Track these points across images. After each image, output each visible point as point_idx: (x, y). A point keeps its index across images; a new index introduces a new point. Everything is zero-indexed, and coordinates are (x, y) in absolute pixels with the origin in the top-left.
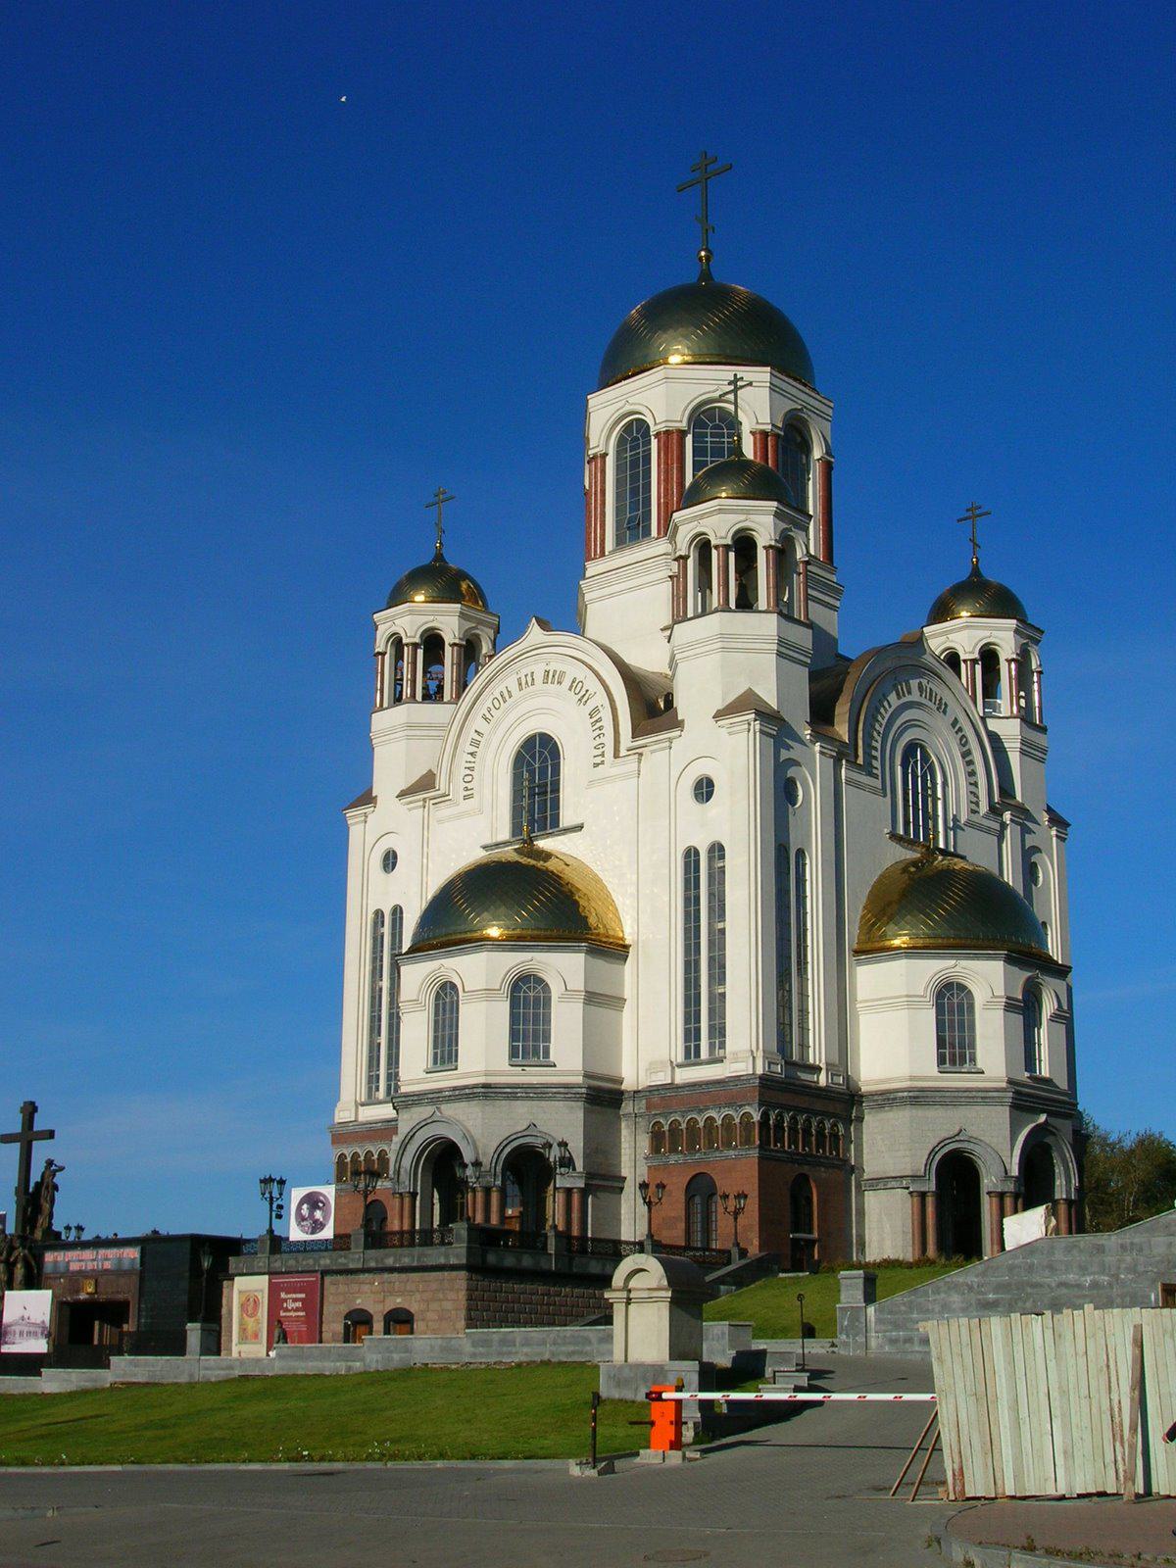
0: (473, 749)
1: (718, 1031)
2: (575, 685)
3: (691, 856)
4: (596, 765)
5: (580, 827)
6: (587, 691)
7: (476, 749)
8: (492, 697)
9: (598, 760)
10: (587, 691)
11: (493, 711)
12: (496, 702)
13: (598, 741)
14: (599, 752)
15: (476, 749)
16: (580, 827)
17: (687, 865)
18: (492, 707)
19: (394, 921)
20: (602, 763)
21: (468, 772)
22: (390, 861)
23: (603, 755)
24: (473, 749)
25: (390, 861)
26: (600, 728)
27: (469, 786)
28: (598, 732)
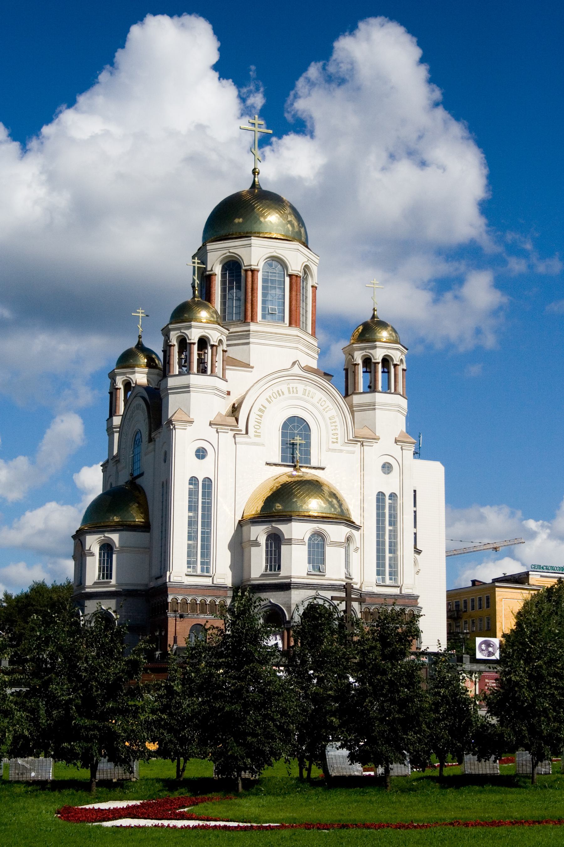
0: (260, 413)
1: (394, 574)
2: (321, 401)
3: (380, 496)
4: (333, 442)
5: (323, 469)
6: (328, 406)
7: (262, 414)
8: (272, 391)
9: (335, 440)
10: (328, 406)
11: (272, 398)
12: (274, 394)
13: (334, 432)
14: (335, 437)
15: (262, 414)
16: (323, 469)
17: (378, 500)
18: (272, 396)
19: (204, 486)
20: (337, 442)
21: (257, 424)
22: (201, 454)
23: (337, 438)
24: (260, 413)
25: (201, 454)
26: (336, 426)
27: (258, 431)
28: (334, 428)
